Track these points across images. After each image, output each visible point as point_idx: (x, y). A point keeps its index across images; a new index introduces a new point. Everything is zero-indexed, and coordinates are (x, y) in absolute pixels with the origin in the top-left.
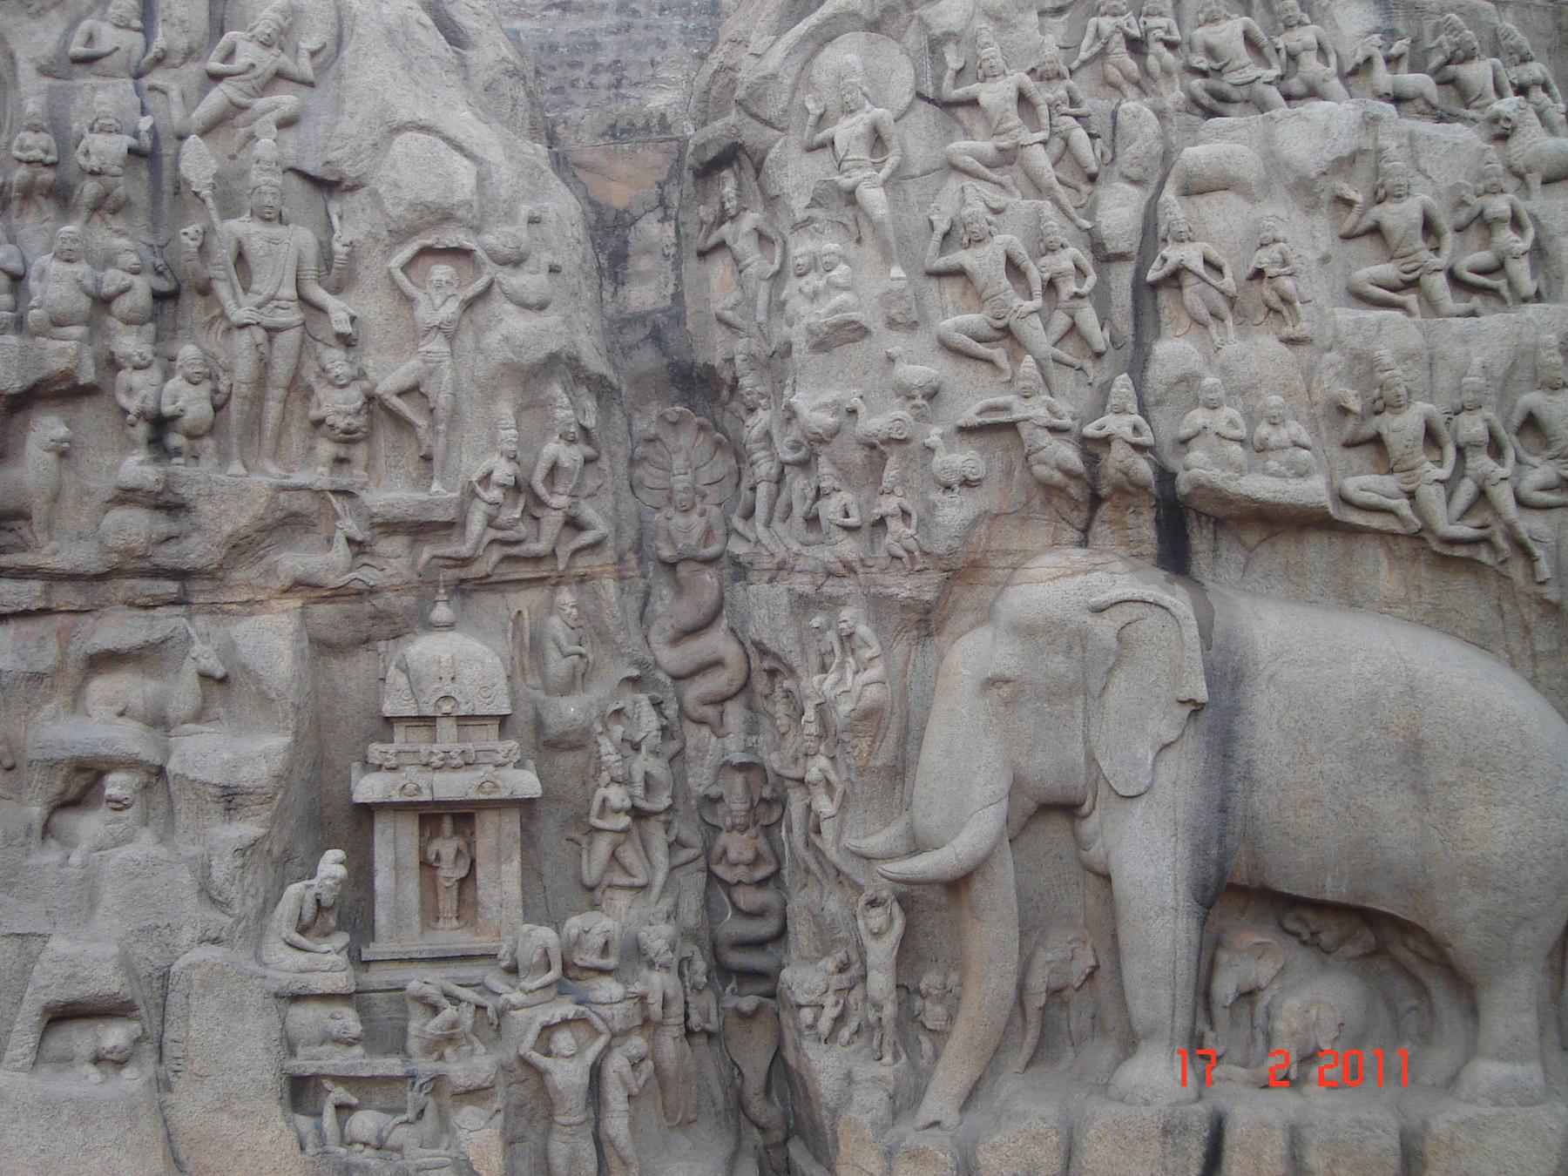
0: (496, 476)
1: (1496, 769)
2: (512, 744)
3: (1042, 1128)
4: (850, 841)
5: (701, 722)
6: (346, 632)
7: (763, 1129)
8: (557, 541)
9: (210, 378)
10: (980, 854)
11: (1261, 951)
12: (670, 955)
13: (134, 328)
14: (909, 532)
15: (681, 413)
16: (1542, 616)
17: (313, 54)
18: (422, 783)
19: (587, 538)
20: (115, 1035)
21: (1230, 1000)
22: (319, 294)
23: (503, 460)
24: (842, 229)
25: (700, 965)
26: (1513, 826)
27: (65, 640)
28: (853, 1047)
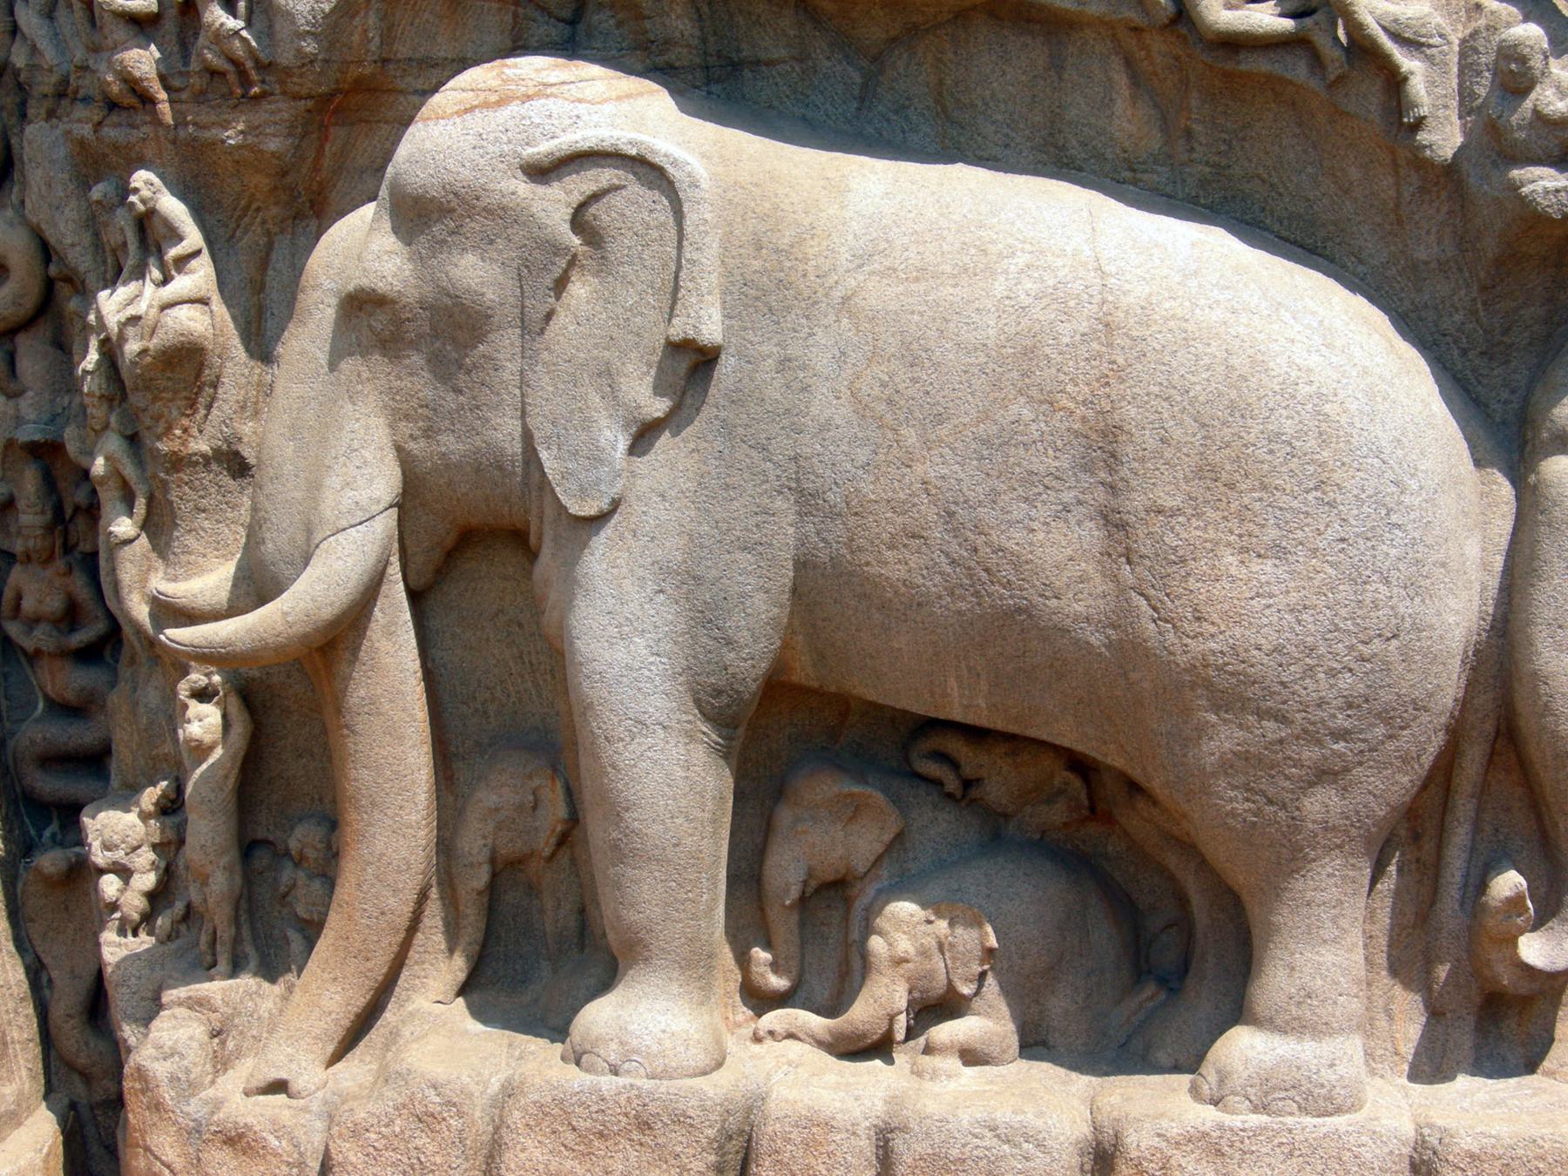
1: (1264, 487)
7: (86, 1078)
10: (327, 613)
11: (854, 810)
14: (232, 23)
16: (1423, 190)
21: (795, 892)
26: (1294, 597)
28: (179, 942)
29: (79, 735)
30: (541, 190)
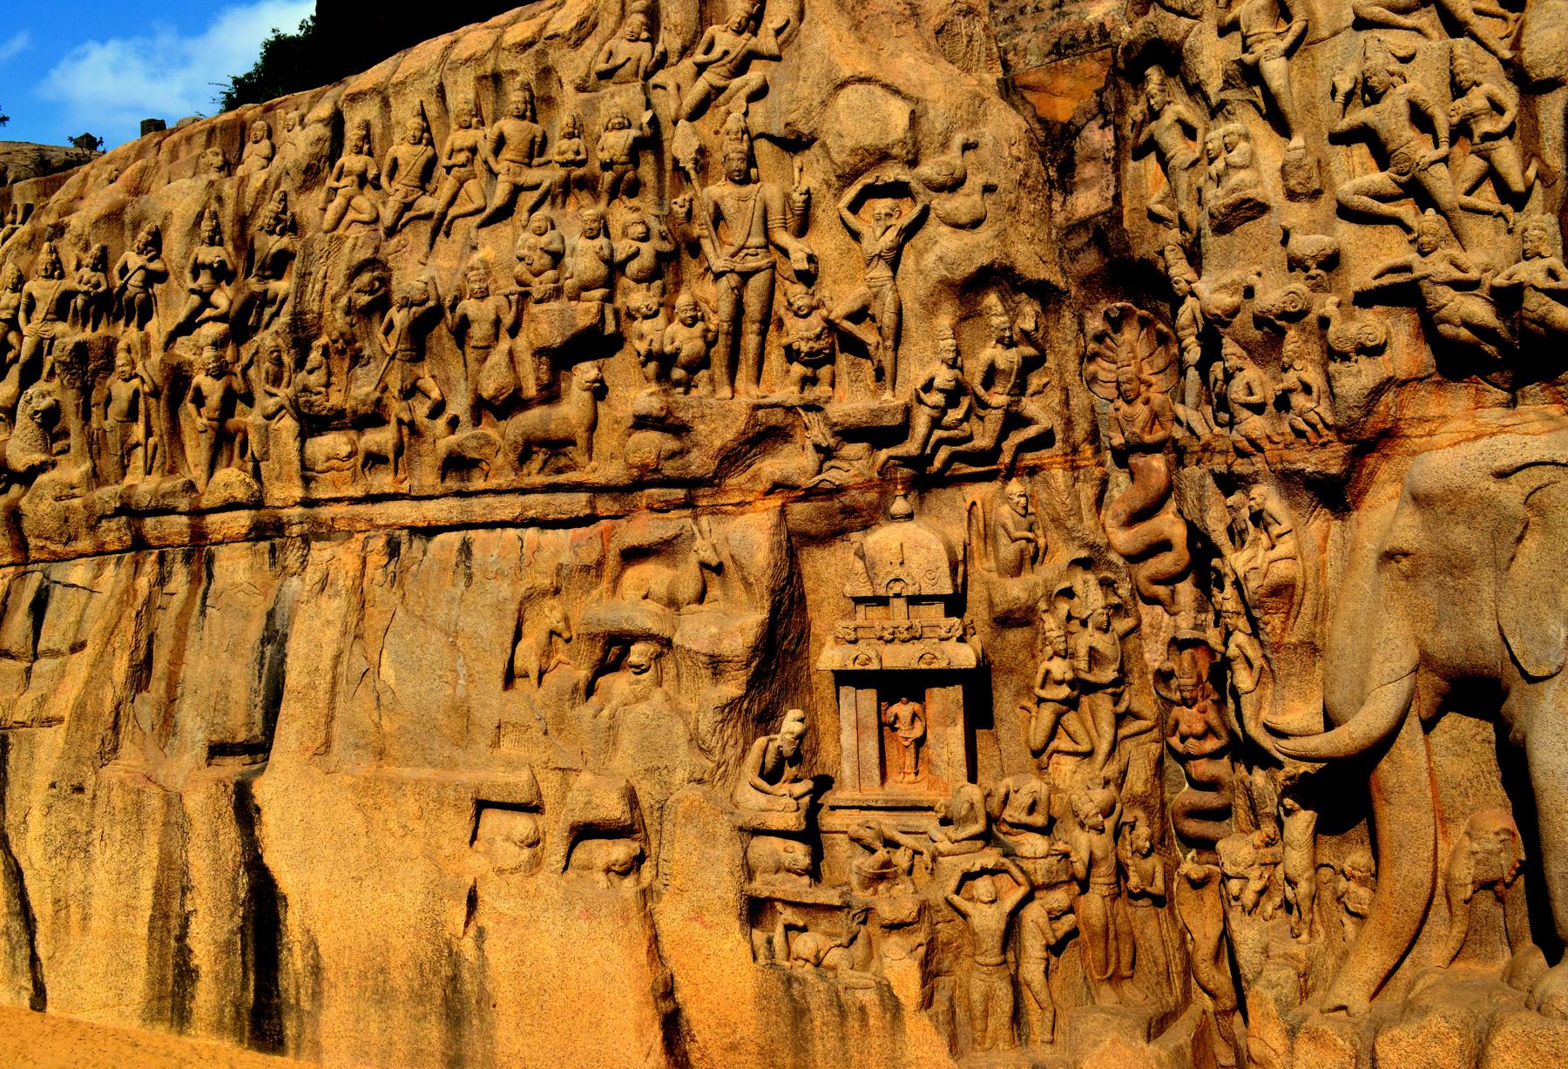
0: (937, 383)
2: (955, 620)
3: (1444, 1027)
4: (1265, 715)
5: (1152, 600)
6: (822, 526)
7: (1213, 995)
8: (1003, 435)
9: (703, 319)
12: (1100, 818)
13: (644, 285)
15: (1121, 309)
17: (778, 32)
18: (872, 654)
19: (1031, 432)
20: (620, 851)
22: (784, 238)
23: (944, 367)
24: (1251, 107)
25: (1143, 830)
27: (606, 537)
29: (1210, 799)
30: (1505, 487)
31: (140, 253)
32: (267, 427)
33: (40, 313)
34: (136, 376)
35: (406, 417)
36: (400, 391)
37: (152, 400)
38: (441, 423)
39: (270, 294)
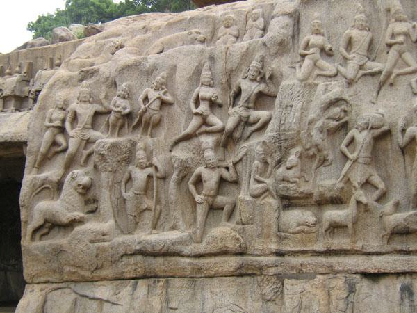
31: (157, 89)
32: (254, 203)
33: (80, 125)
34: (151, 165)
35: (364, 200)
36: (359, 184)
37: (161, 182)
38: (388, 206)
39: (251, 119)
